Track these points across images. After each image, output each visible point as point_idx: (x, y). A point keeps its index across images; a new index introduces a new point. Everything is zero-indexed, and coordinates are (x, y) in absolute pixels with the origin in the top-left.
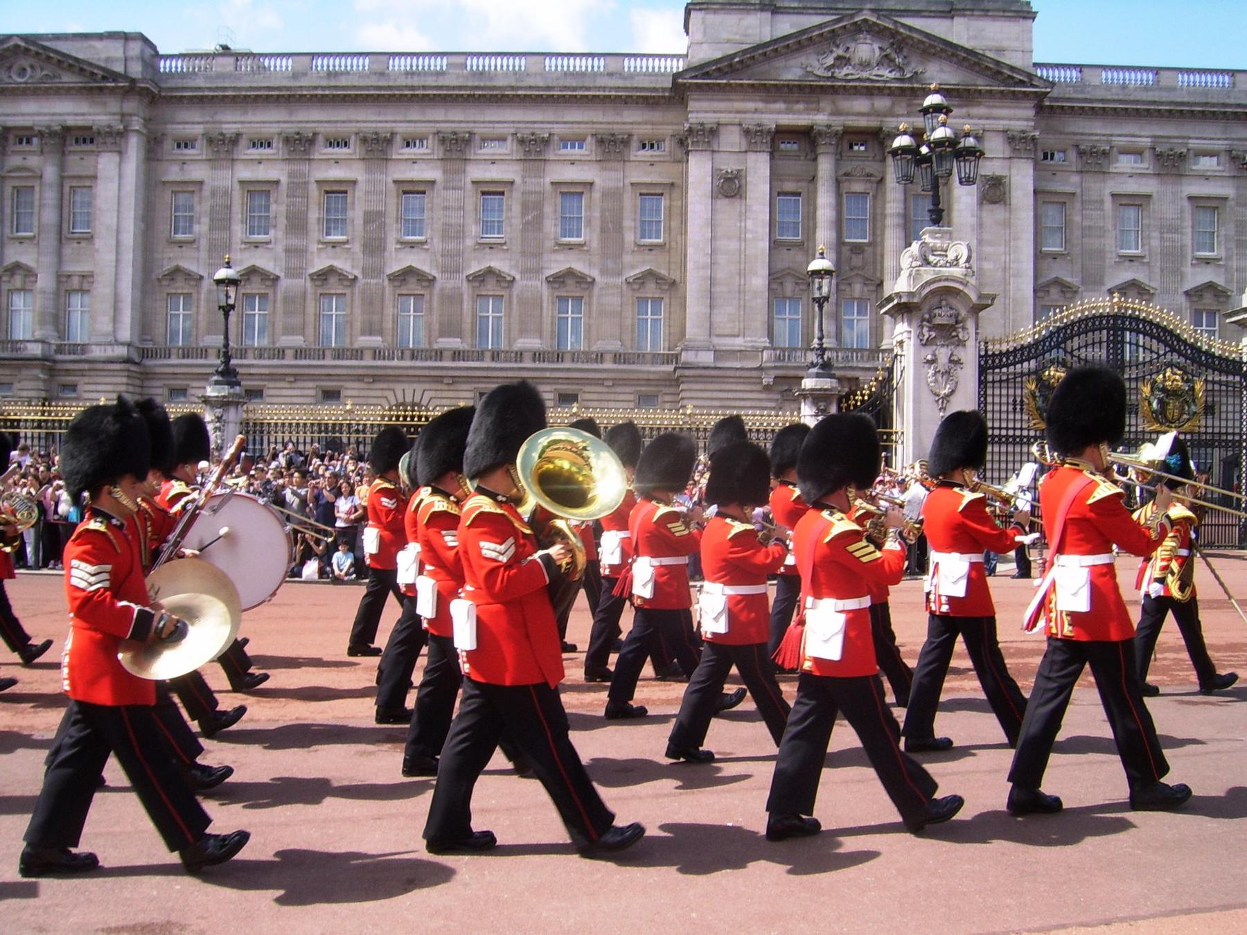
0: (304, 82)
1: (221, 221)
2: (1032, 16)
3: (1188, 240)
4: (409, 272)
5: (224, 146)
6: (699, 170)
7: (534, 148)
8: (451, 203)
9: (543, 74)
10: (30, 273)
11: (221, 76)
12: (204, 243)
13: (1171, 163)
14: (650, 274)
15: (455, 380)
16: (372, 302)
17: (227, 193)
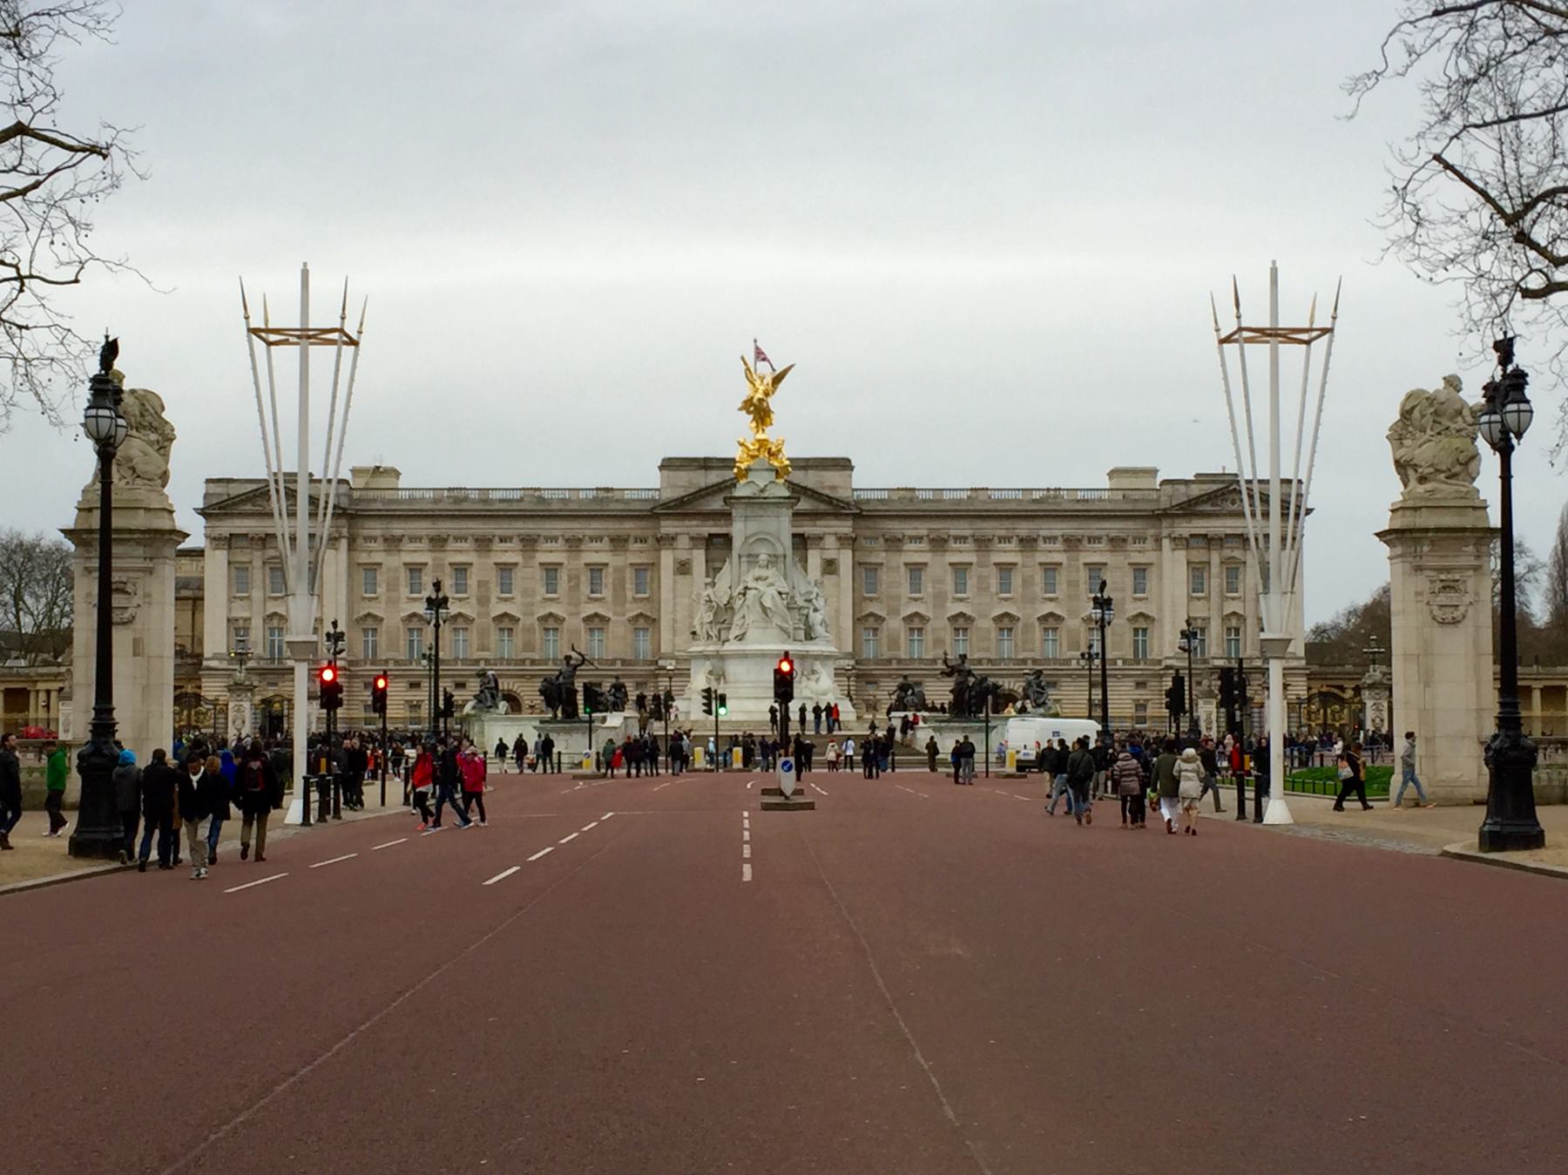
0: (440, 506)
1: (393, 586)
2: (852, 468)
3: (949, 586)
4: (505, 615)
5: (393, 543)
6: (667, 558)
7: (574, 544)
8: (529, 577)
9: (579, 501)
10: (282, 617)
11: (391, 501)
12: (383, 599)
13: (939, 544)
14: (641, 615)
15: (533, 676)
16: (483, 633)
17: (396, 569)
